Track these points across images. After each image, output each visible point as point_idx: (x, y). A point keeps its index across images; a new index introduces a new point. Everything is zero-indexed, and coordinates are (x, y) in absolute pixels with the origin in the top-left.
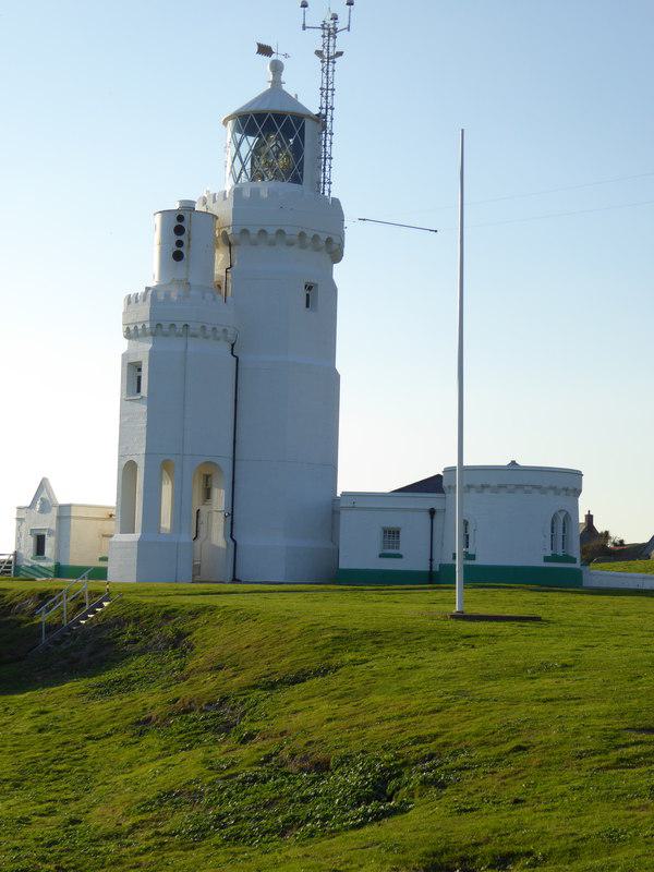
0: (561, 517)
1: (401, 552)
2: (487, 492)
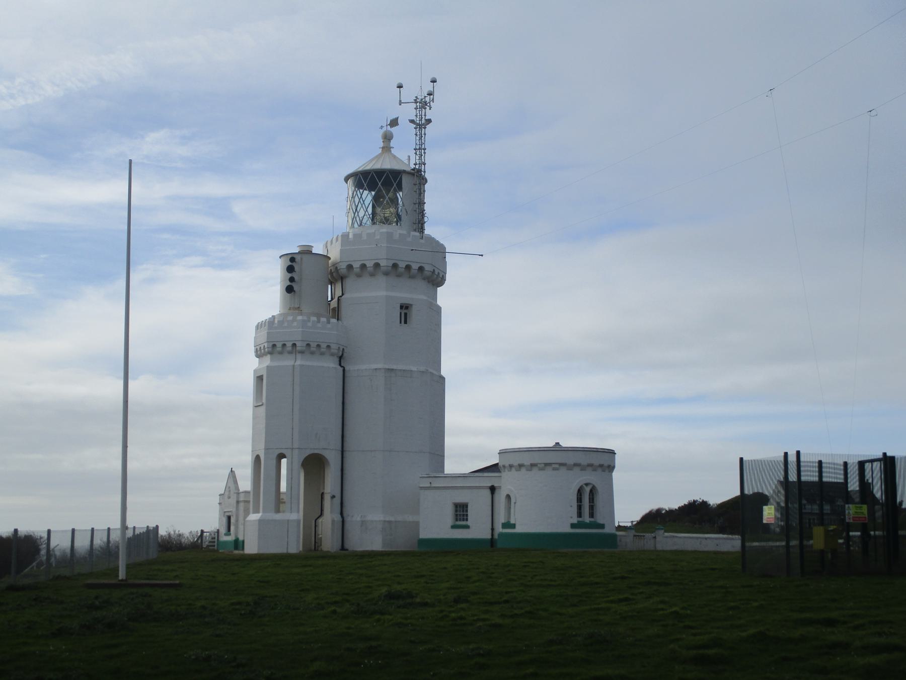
0: (588, 489)
1: (469, 523)
2: (523, 470)
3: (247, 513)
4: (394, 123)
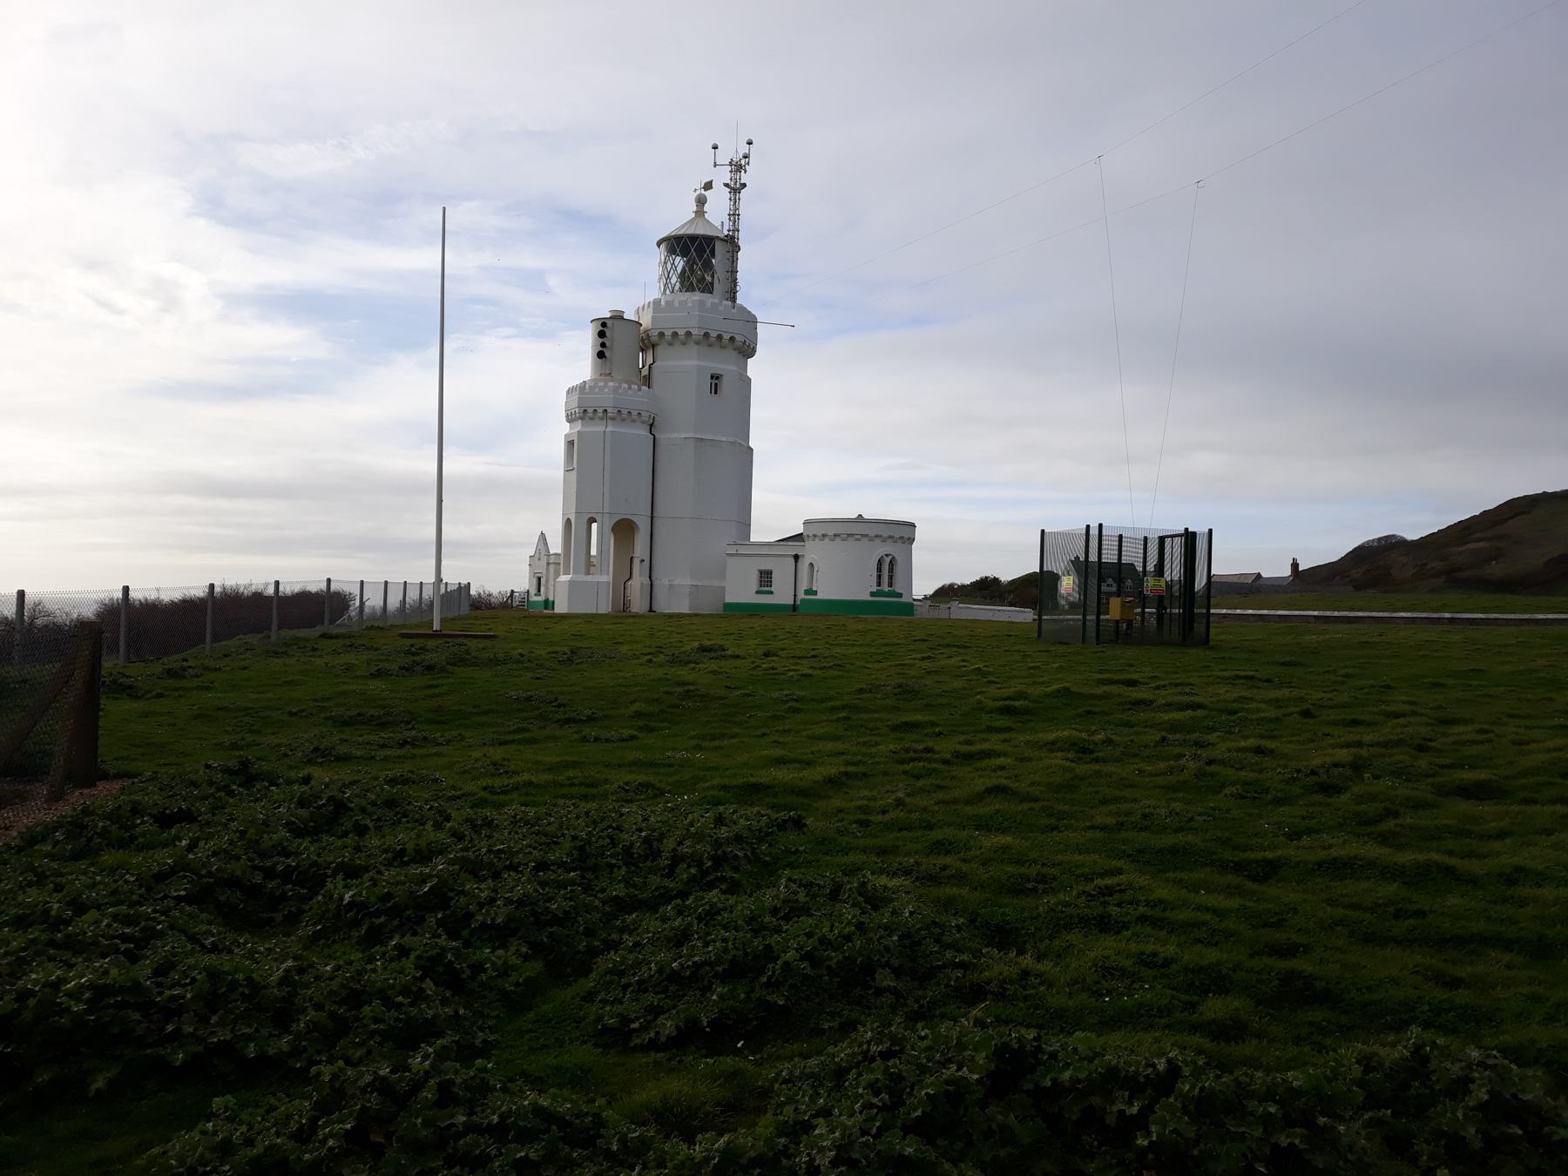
3: (557, 575)
4: (708, 186)
